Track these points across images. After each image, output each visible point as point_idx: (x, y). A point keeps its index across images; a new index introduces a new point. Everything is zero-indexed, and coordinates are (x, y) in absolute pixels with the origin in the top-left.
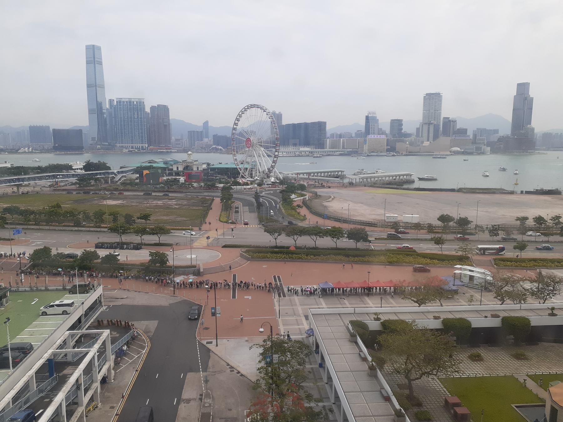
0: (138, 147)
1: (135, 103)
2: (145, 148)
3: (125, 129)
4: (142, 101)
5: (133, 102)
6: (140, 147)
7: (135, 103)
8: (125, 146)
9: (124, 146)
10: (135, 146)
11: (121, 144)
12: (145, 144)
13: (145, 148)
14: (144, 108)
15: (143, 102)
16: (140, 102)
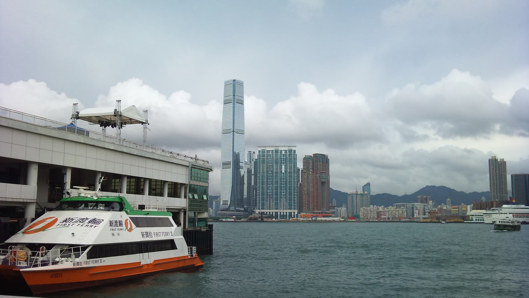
0: (285, 214)
1: (283, 152)
2: (294, 215)
3: (267, 189)
4: (294, 149)
5: (281, 151)
6: (286, 214)
7: (283, 152)
8: (267, 212)
9: (265, 213)
10: (280, 212)
11: (262, 209)
12: (295, 209)
13: (294, 215)
14: (295, 159)
15: (295, 151)
16: (290, 151)
